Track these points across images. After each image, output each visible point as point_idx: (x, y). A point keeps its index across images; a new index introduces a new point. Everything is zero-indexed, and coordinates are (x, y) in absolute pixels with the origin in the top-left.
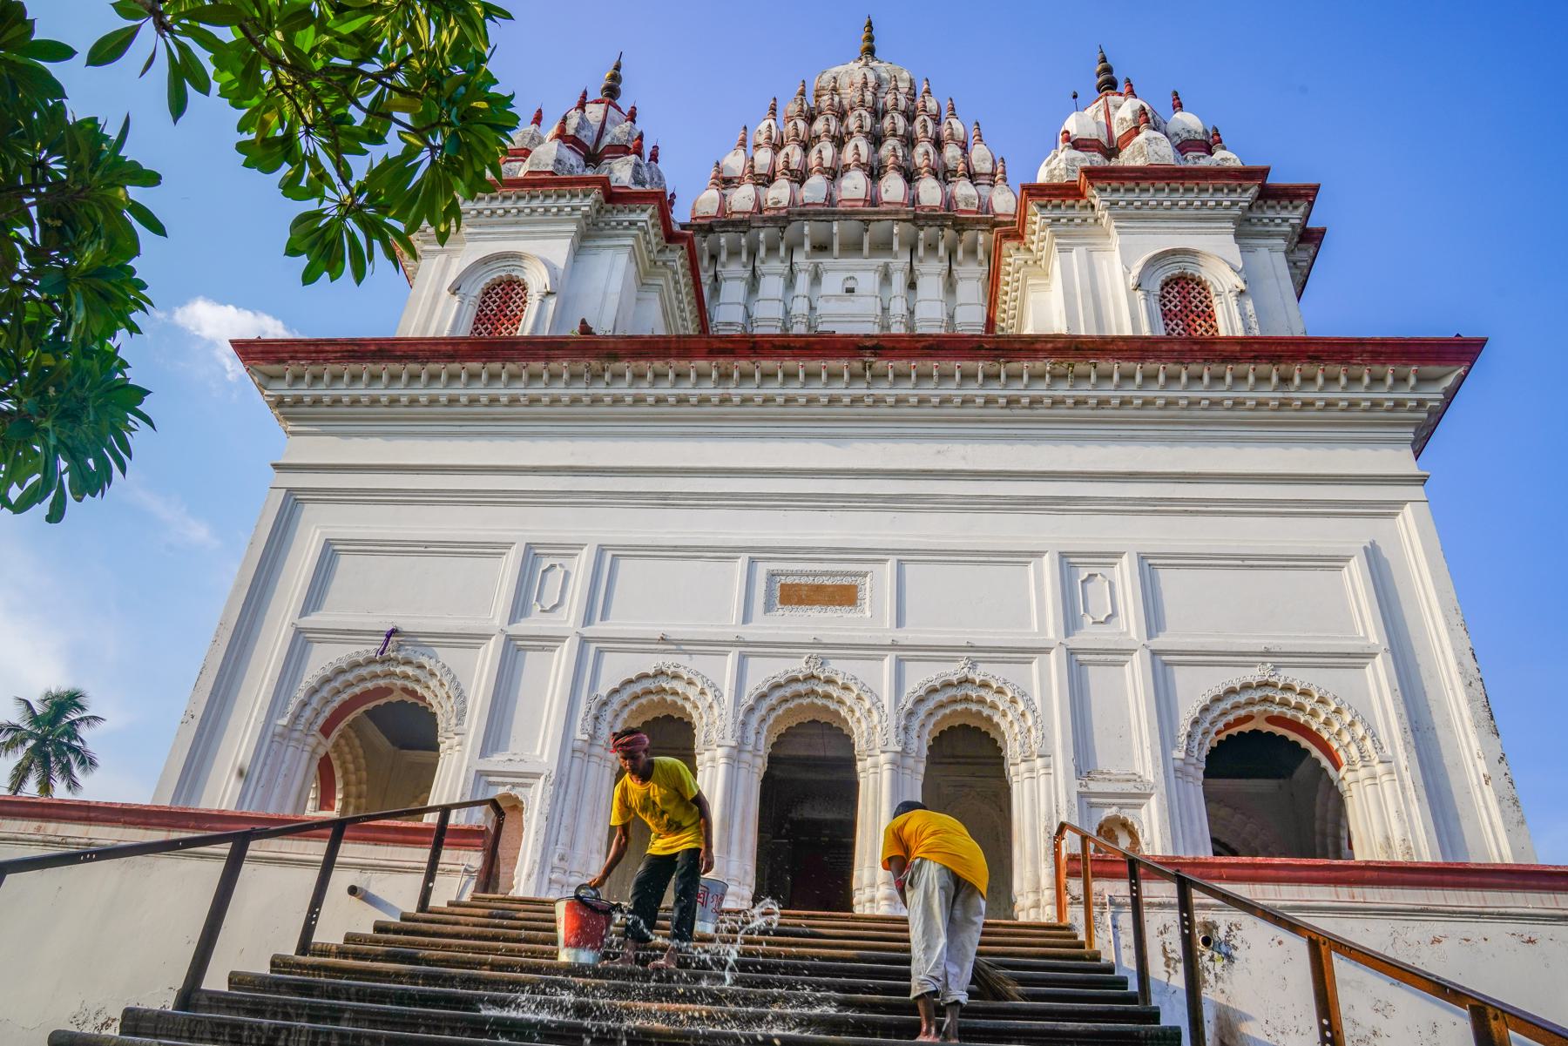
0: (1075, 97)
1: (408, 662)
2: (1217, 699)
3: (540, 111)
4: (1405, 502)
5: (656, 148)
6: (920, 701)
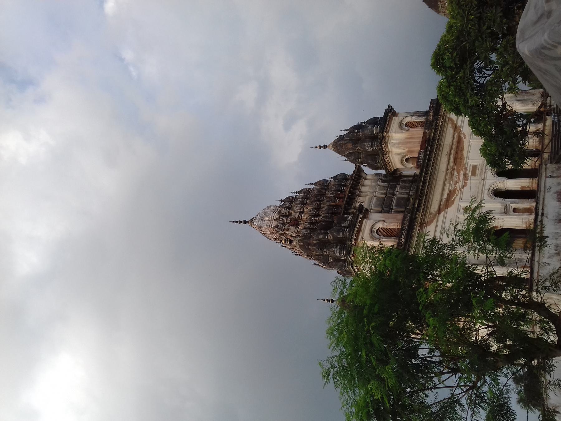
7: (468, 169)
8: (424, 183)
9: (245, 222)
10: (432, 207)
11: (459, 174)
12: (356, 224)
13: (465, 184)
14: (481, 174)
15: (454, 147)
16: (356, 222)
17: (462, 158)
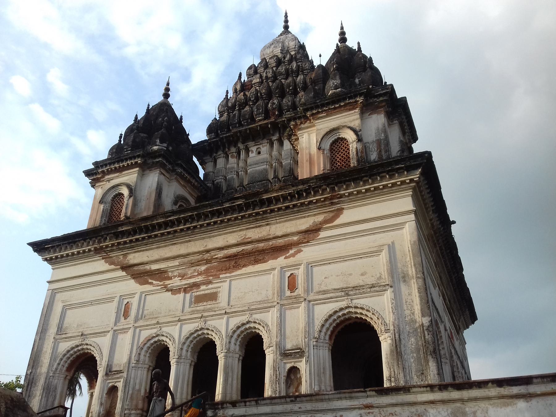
0: (320, 56)
1: (87, 344)
2: (331, 316)
3: (137, 115)
4: (406, 222)
5: (181, 116)
6: (234, 332)
7: (210, 286)
8: (166, 225)
9: (286, 27)
10: (137, 255)
11: (200, 274)
12: (122, 161)
13: (174, 291)
14: (193, 312)
15: (261, 245)
16: (126, 160)
17: (237, 267)
